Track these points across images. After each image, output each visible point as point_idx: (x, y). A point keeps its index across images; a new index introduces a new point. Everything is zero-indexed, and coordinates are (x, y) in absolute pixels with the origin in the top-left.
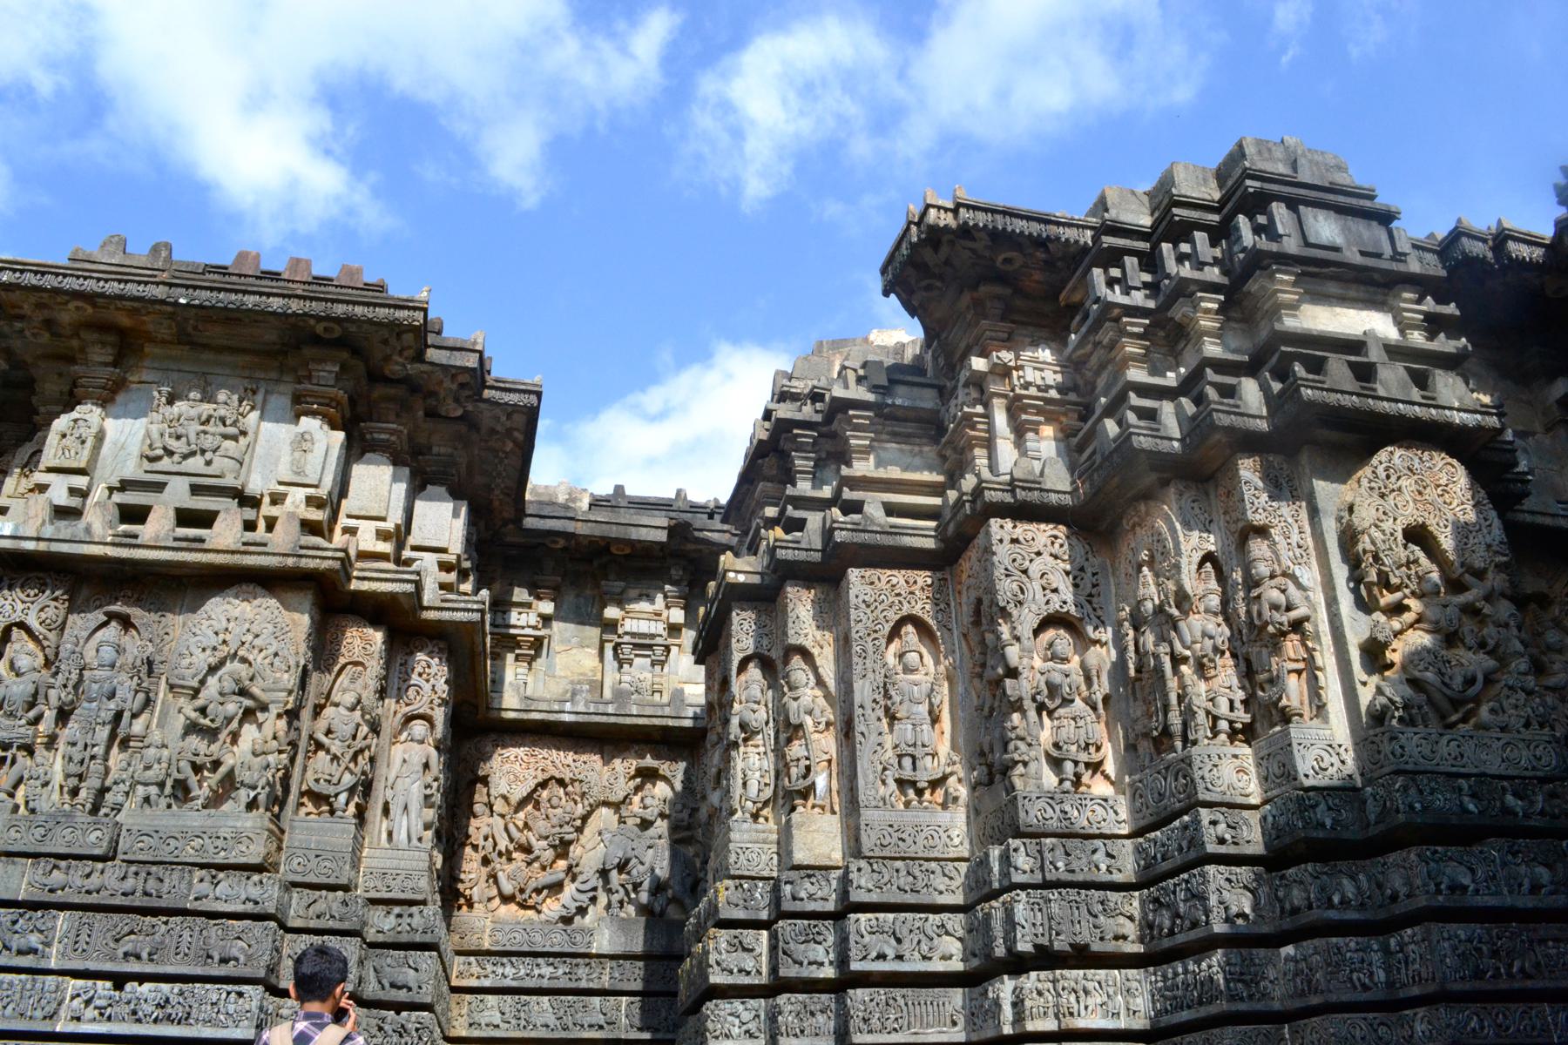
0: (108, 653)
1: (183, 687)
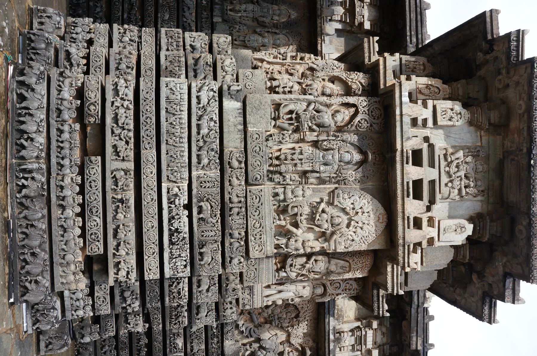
0: (347, 157)
1: (333, 198)
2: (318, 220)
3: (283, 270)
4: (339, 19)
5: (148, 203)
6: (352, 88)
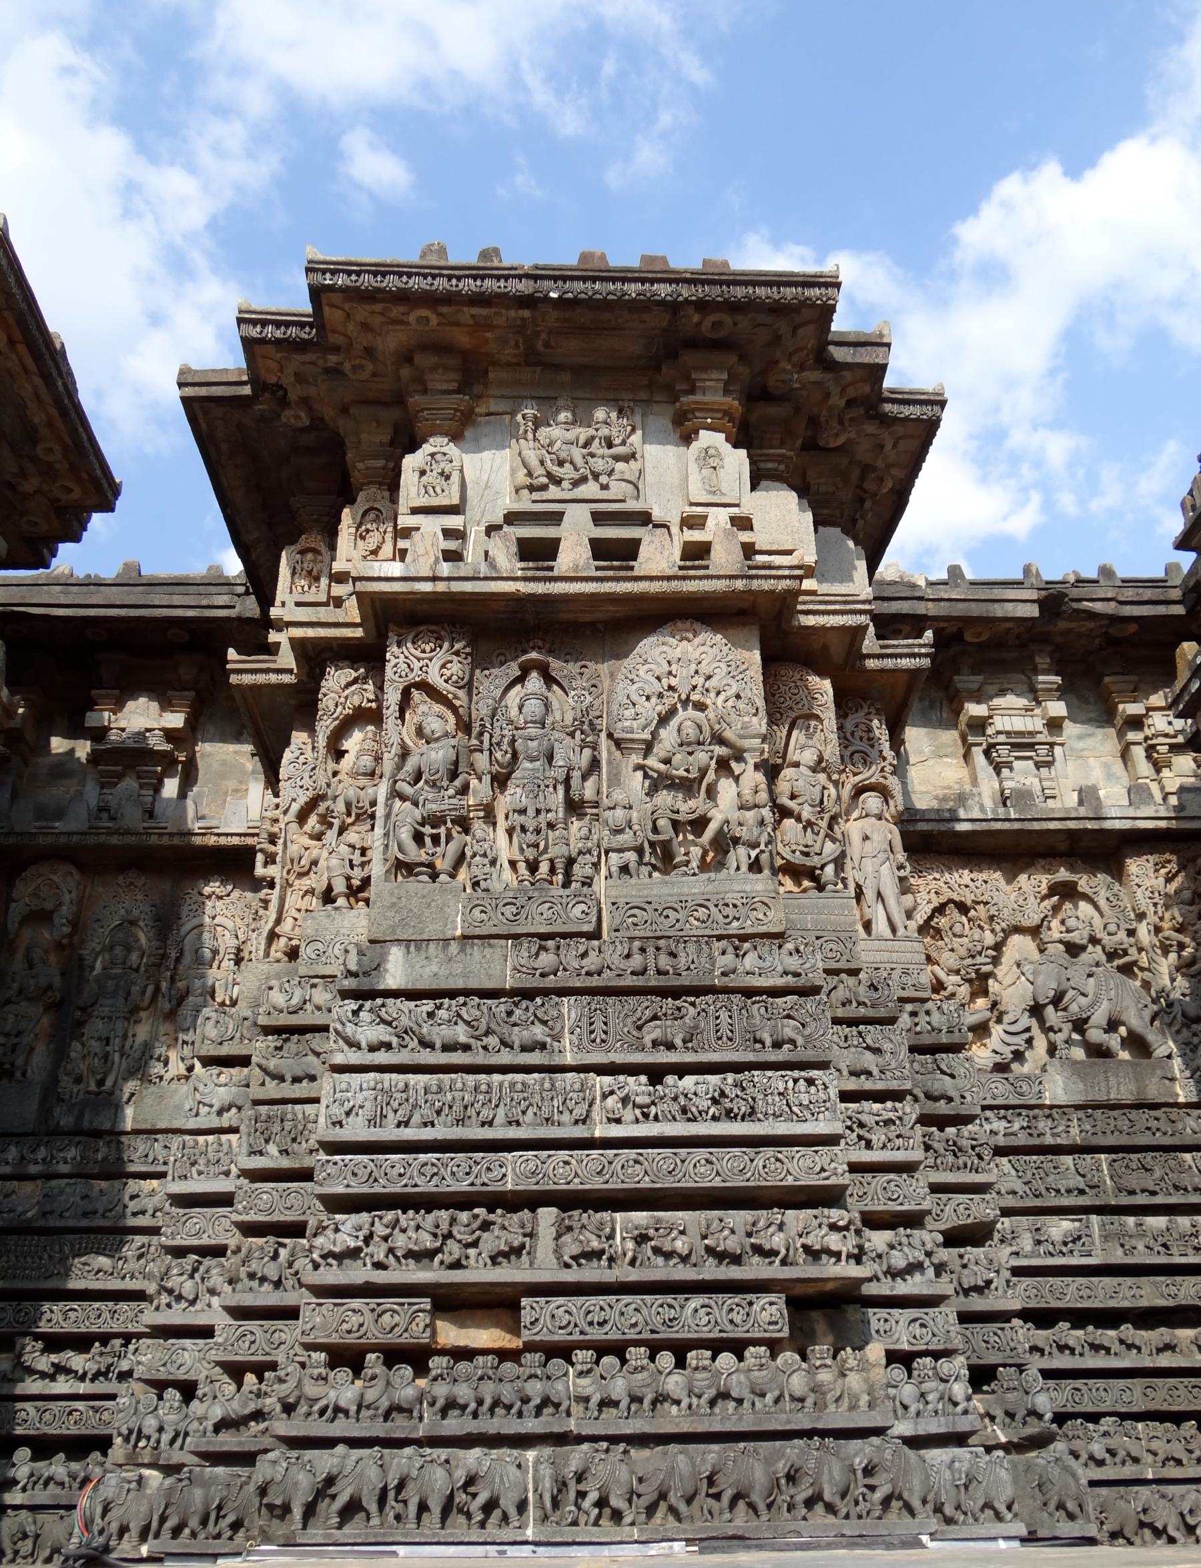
0: (533, 706)
1: (632, 741)
2: (687, 771)
3: (818, 872)
4: (151, 792)
5: (646, 1172)
6: (360, 706)
